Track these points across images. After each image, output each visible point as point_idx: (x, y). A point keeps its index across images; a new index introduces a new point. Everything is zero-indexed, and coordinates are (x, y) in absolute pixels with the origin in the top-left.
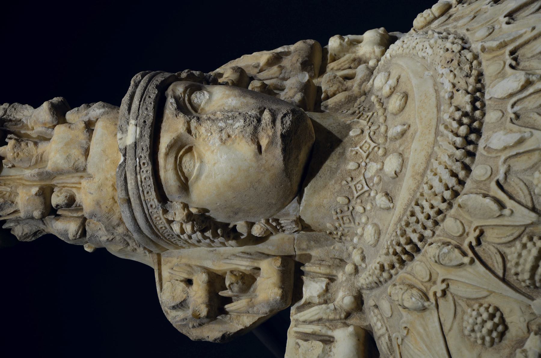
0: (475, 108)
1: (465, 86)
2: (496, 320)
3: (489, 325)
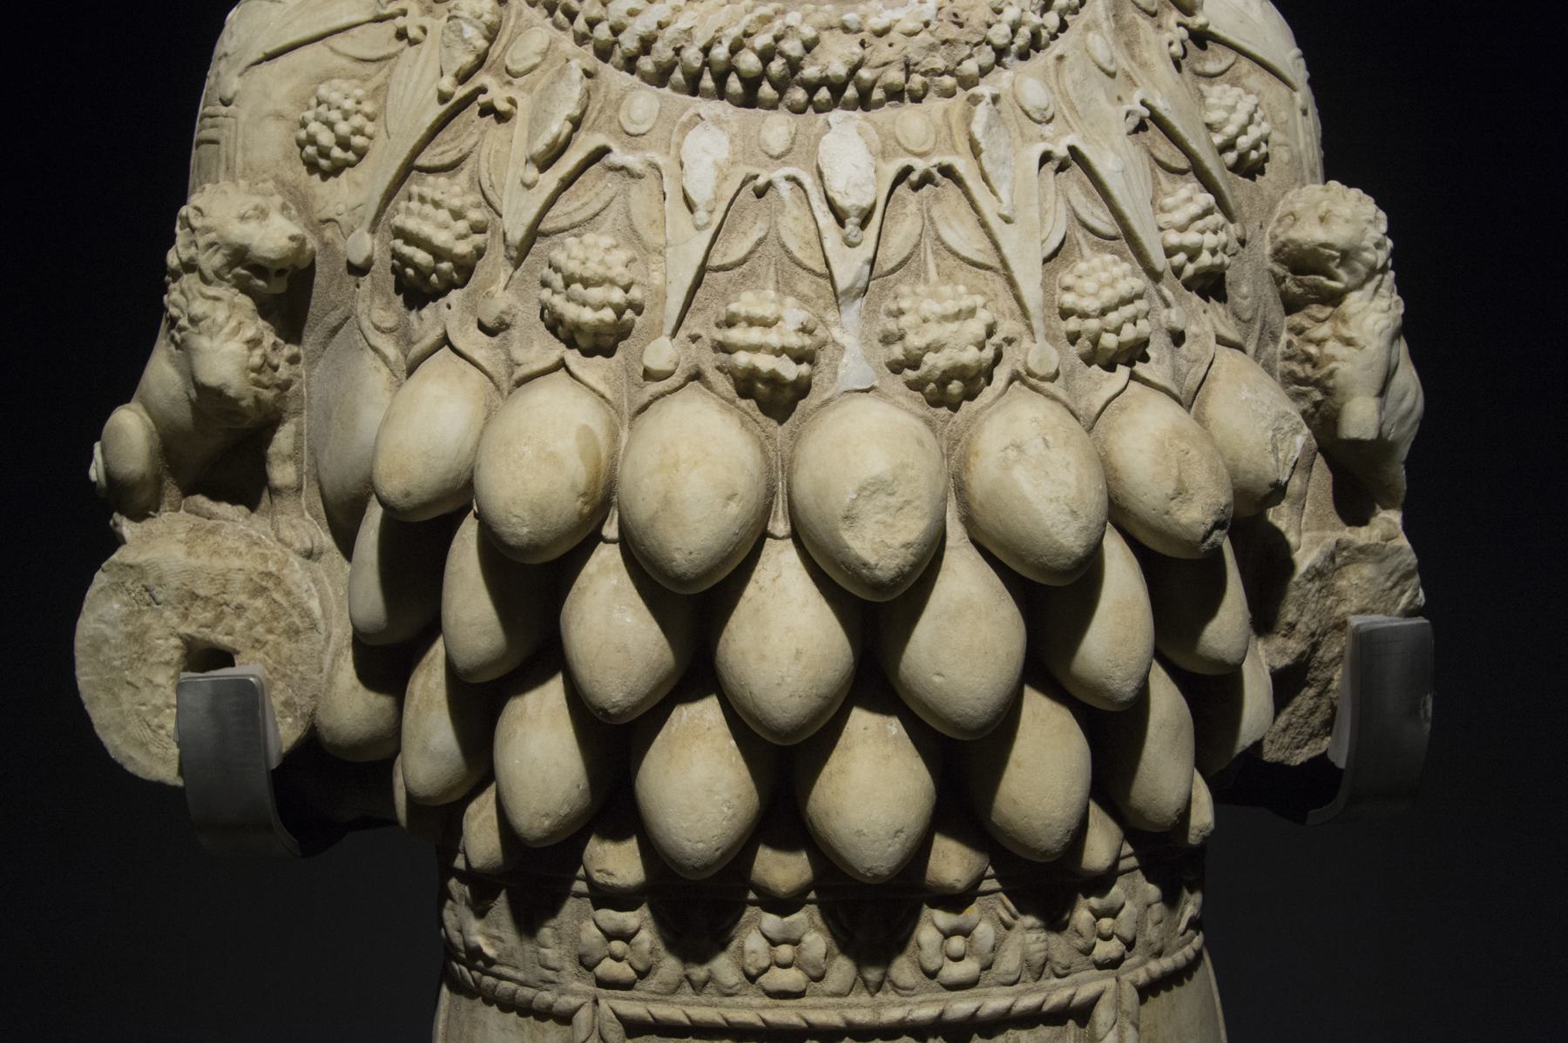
0: (811, 88)
1: (876, 59)
2: (337, 152)
3: (326, 138)
